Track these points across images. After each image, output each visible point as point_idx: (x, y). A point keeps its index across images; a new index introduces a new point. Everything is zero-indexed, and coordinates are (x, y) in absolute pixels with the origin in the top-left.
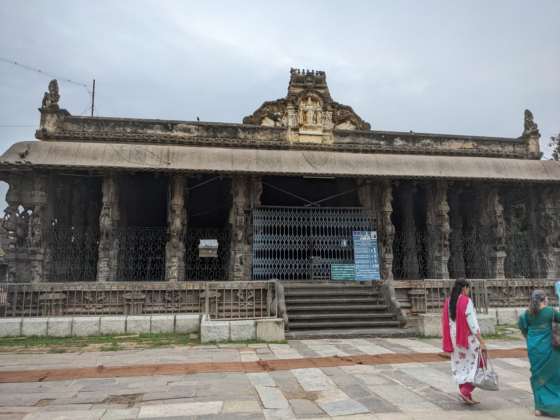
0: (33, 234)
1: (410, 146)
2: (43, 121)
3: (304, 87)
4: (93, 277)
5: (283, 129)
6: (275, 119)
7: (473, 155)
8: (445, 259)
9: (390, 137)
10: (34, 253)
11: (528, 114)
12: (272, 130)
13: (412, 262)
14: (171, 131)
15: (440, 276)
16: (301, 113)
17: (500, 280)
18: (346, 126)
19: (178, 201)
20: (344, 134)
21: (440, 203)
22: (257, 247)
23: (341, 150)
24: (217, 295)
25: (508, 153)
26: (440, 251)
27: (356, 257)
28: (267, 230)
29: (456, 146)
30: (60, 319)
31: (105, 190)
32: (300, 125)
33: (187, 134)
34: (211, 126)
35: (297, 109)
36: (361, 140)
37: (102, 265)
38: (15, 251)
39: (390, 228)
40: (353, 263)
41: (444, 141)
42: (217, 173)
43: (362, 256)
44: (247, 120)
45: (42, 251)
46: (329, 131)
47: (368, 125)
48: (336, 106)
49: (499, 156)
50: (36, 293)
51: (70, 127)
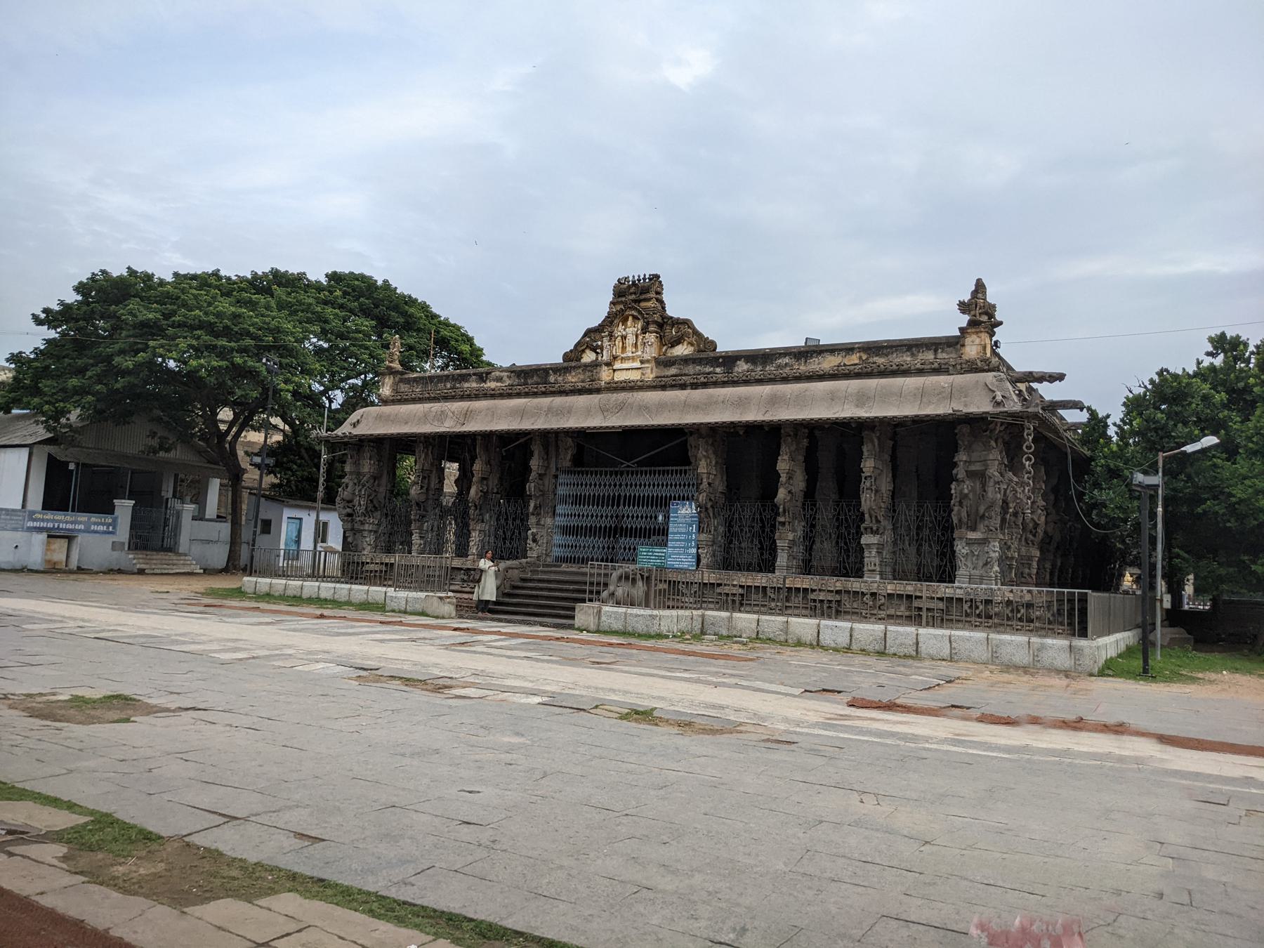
7: (858, 375)
9: (730, 360)
13: (826, 549)
16: (618, 342)
18: (682, 350)
22: (560, 521)
23: (663, 388)
25: (919, 366)
29: (829, 363)
32: (615, 358)
36: (691, 369)
40: (664, 544)
41: (811, 357)
43: (677, 537)
44: (567, 357)
46: (648, 361)
47: (713, 346)
49: (906, 372)
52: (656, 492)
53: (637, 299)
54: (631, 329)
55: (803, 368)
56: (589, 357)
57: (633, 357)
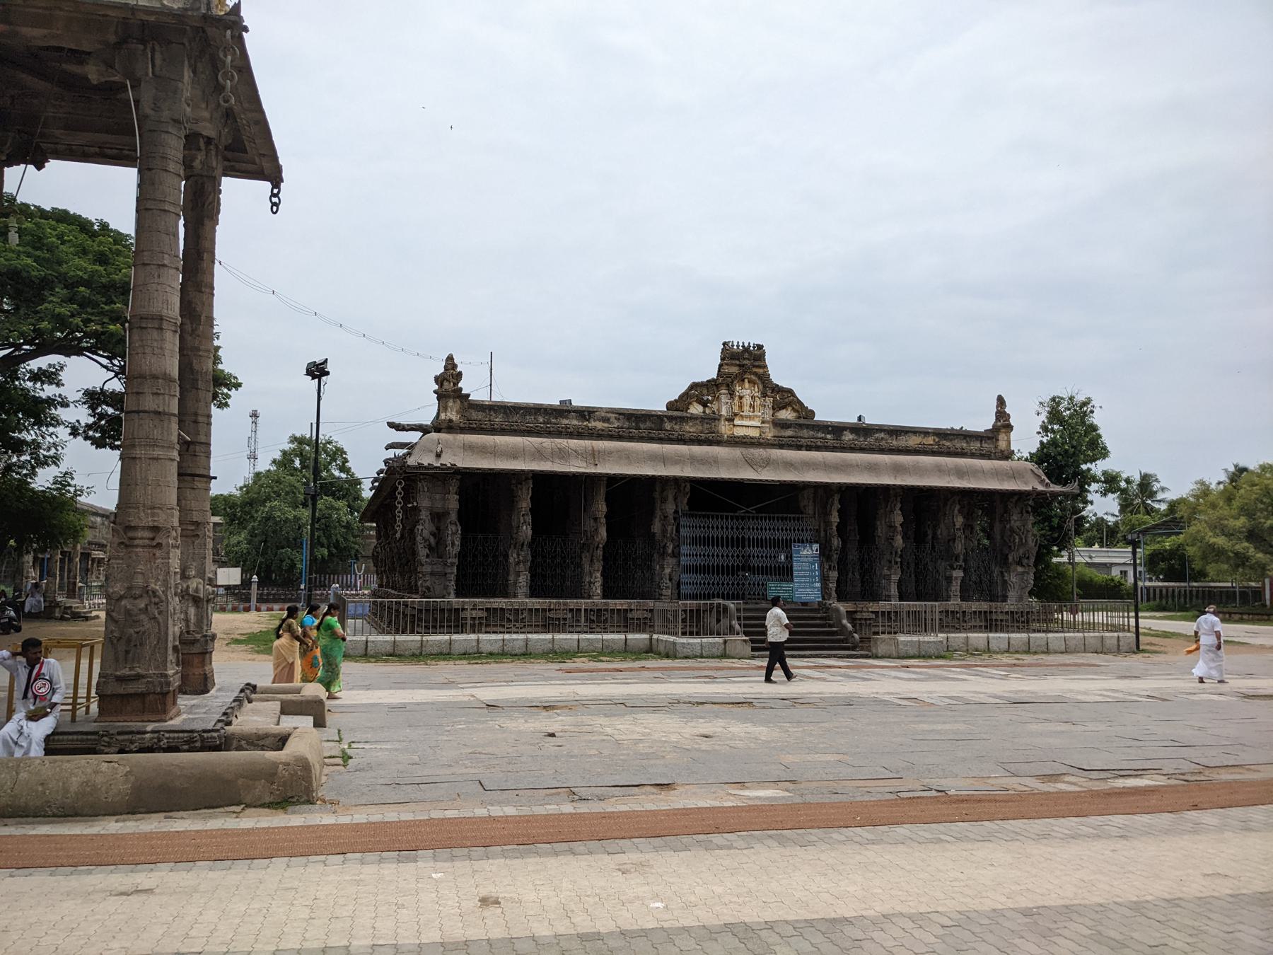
0: (453, 544)
1: (861, 441)
5: (715, 418)
6: (705, 405)
8: (895, 578)
9: (837, 429)
11: (1001, 401)
12: (703, 419)
15: (888, 598)
17: (955, 603)
18: (786, 414)
20: (783, 425)
21: (892, 511)
22: (684, 561)
23: (781, 446)
26: (889, 568)
27: (795, 574)
28: (696, 541)
29: (913, 441)
32: (736, 415)
34: (632, 415)
36: (805, 433)
39: (836, 542)
40: (792, 581)
43: (802, 574)
44: (671, 406)
47: (813, 413)
48: (777, 389)
49: (962, 454)
50: (457, 610)
51: (476, 415)
52: (777, 535)
53: (743, 363)
56: (696, 409)
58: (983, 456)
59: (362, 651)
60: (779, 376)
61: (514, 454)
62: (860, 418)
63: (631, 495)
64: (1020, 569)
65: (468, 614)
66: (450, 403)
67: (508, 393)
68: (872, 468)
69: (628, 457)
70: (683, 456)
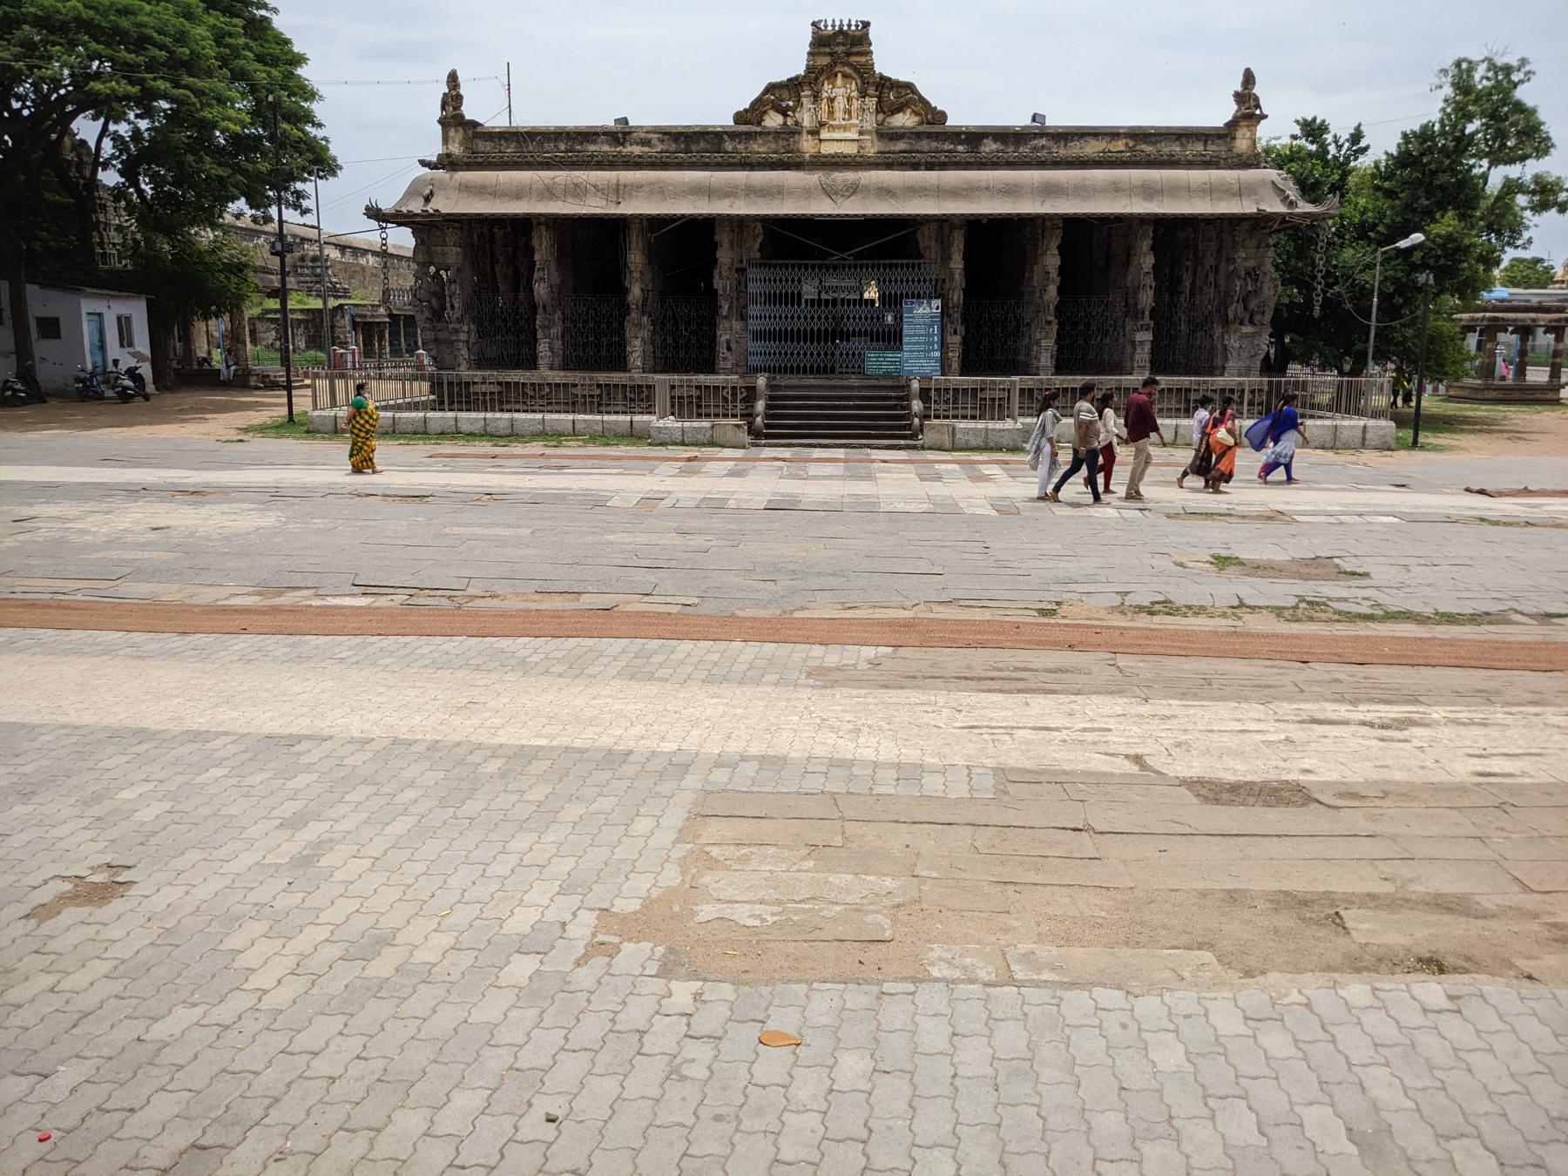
0: (452, 306)
1: (1011, 152)
2: (445, 140)
3: (831, 54)
4: (531, 363)
6: (785, 115)
9: (974, 137)
10: (456, 331)
11: (1249, 78)
12: (776, 134)
14: (622, 145)
16: (824, 105)
19: (636, 258)
22: (753, 325)
23: (889, 166)
24: (694, 393)
27: (905, 340)
28: (773, 299)
29: (1092, 148)
30: (498, 415)
31: (535, 242)
32: (822, 125)
33: (646, 149)
34: (682, 134)
35: (816, 97)
36: (925, 145)
37: (543, 348)
38: (434, 329)
40: (900, 349)
42: (683, 216)
44: (740, 118)
45: (465, 328)
46: (869, 133)
47: (943, 116)
48: (884, 84)
50: (468, 384)
51: (482, 146)
53: (840, 50)
54: (840, 91)
55: (1062, 151)
56: (773, 120)
57: (844, 124)
58: (1207, 164)
59: (331, 427)
60: (887, 62)
61: (518, 194)
62: (1034, 120)
63: (686, 244)
64: (1247, 329)
65: (578, 391)
66: (452, 133)
67: (532, 115)
68: (1010, 191)
69: (661, 191)
70: (736, 187)
